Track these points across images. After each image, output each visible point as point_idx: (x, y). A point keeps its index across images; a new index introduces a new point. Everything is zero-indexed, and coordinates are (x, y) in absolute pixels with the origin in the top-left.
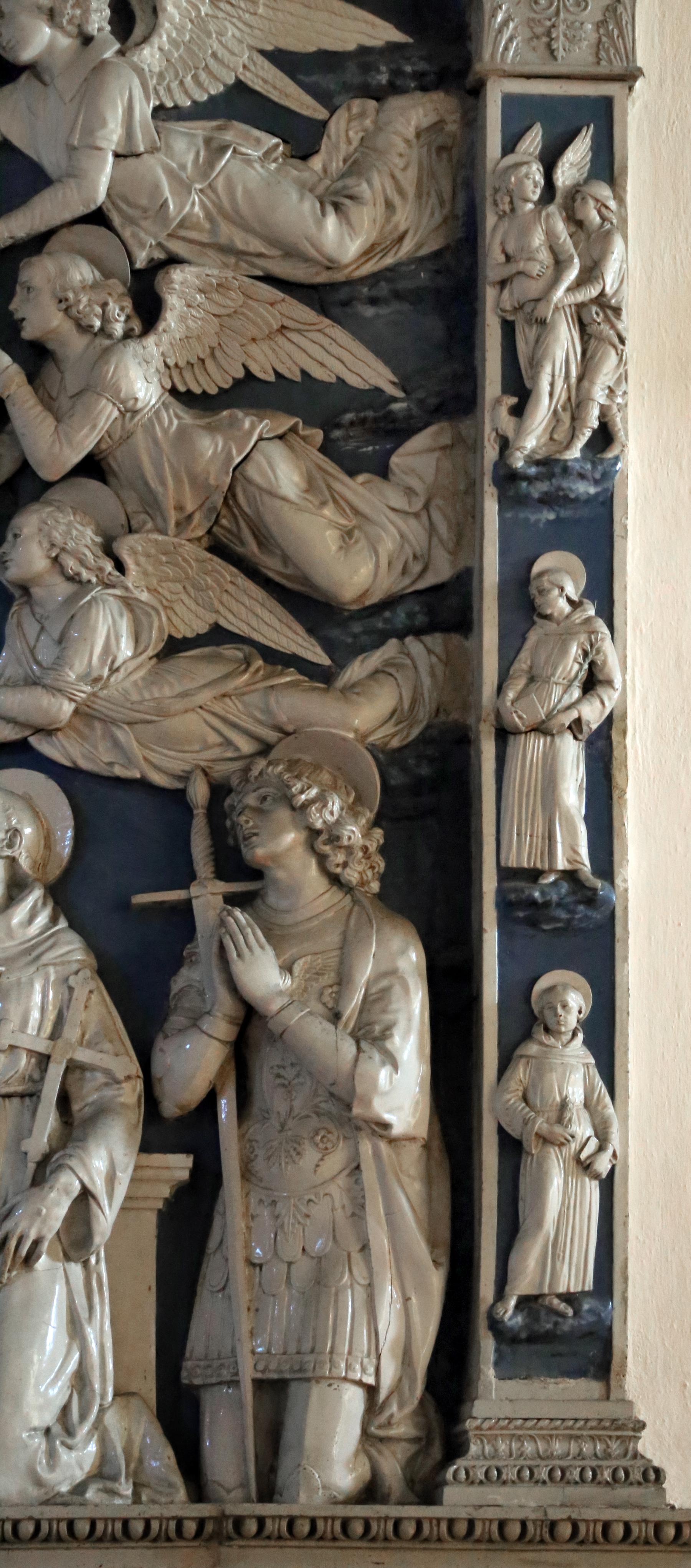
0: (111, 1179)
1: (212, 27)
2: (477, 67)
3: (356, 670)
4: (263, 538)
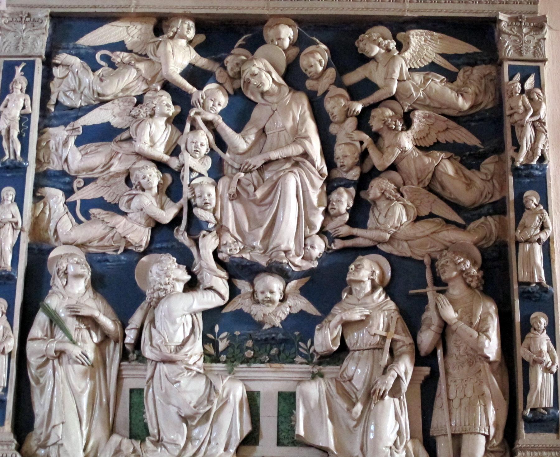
0: (406, 373)
1: (425, 47)
2: (500, 57)
3: (472, 225)
4: (443, 187)
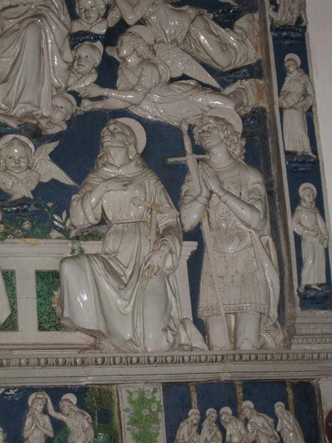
3: (228, 90)
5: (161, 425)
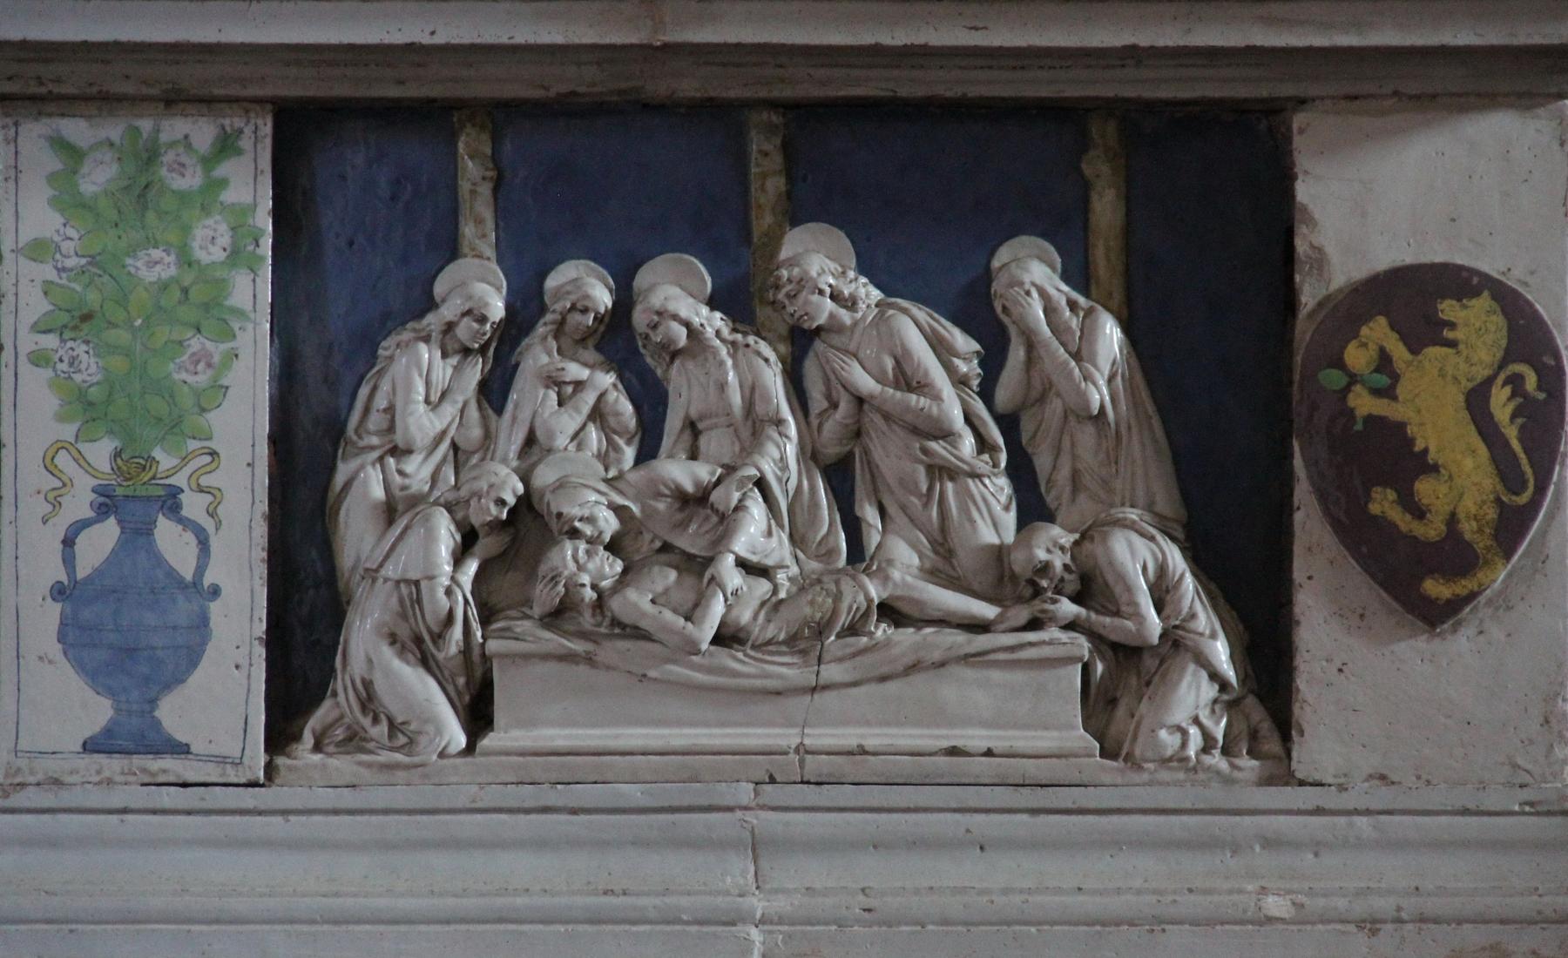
5: (244, 341)
